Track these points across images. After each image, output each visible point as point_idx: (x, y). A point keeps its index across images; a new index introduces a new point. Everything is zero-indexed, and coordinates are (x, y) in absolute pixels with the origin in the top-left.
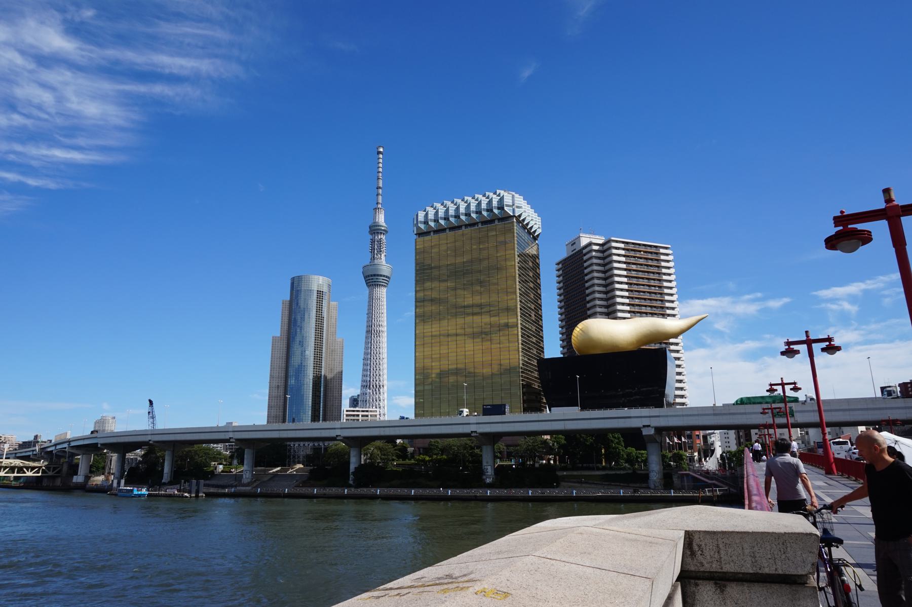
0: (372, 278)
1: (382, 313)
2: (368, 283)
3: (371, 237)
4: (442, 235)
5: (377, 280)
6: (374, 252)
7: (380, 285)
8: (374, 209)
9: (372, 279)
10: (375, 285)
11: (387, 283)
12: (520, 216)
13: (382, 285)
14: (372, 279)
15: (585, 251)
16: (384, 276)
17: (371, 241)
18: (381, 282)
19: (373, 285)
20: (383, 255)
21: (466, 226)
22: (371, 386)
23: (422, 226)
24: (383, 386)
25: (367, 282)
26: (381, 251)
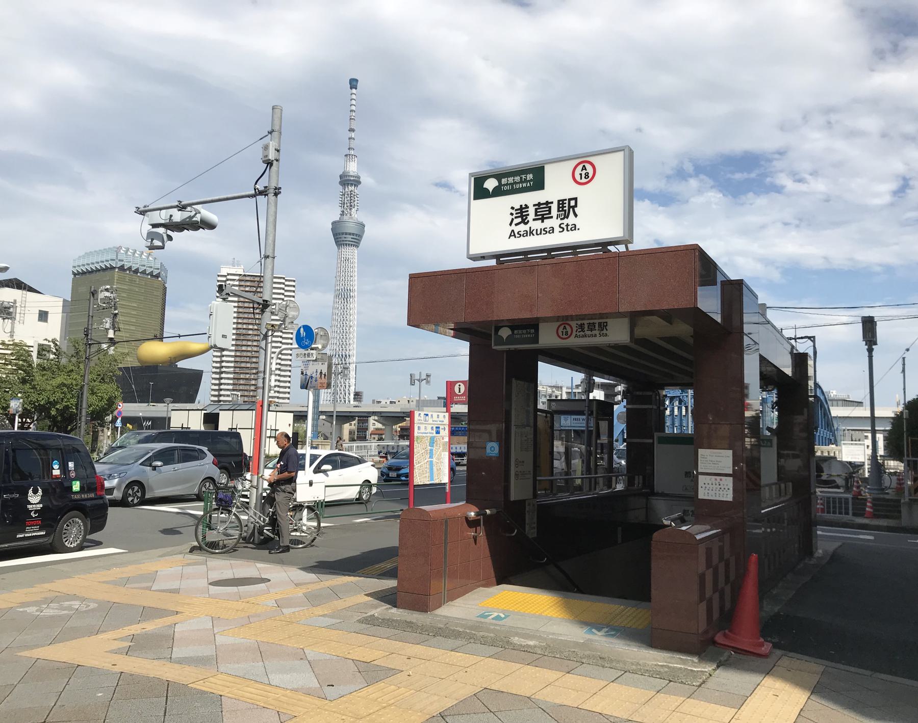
0: (340, 236)
2: (338, 241)
5: (345, 239)
6: (344, 207)
7: (349, 244)
9: (340, 238)
10: (344, 244)
11: (357, 243)
14: (340, 238)
16: (353, 234)
17: (341, 194)
19: (341, 244)
20: (353, 209)
22: (337, 355)
24: (349, 356)
25: (337, 240)
26: (351, 206)
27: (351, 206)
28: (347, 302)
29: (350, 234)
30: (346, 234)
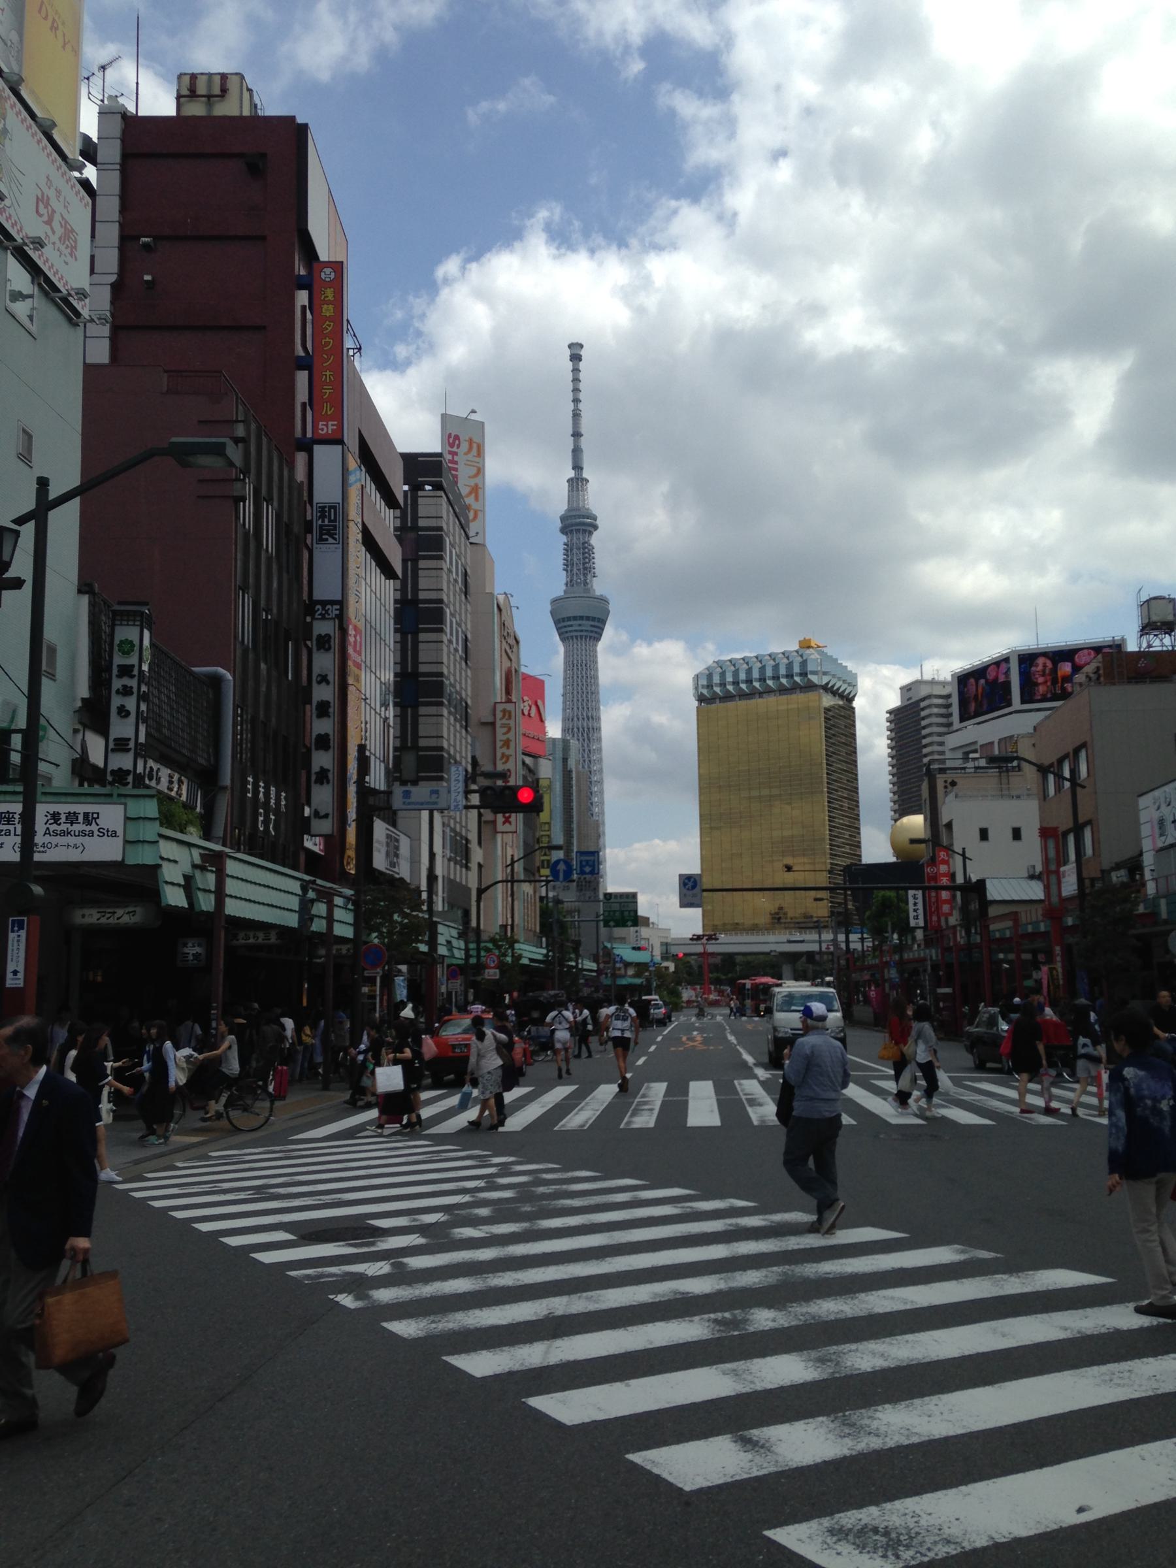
0: (569, 623)
1: (592, 693)
3: (564, 539)
4: (731, 705)
6: (571, 571)
8: (568, 481)
9: (571, 626)
10: (577, 637)
12: (827, 684)
13: (591, 637)
14: (571, 626)
15: (922, 705)
16: (594, 619)
18: (586, 631)
21: (761, 694)
23: (705, 692)
26: (585, 569)
27: (585, 569)
28: (589, 740)
29: (588, 618)
30: (581, 618)
